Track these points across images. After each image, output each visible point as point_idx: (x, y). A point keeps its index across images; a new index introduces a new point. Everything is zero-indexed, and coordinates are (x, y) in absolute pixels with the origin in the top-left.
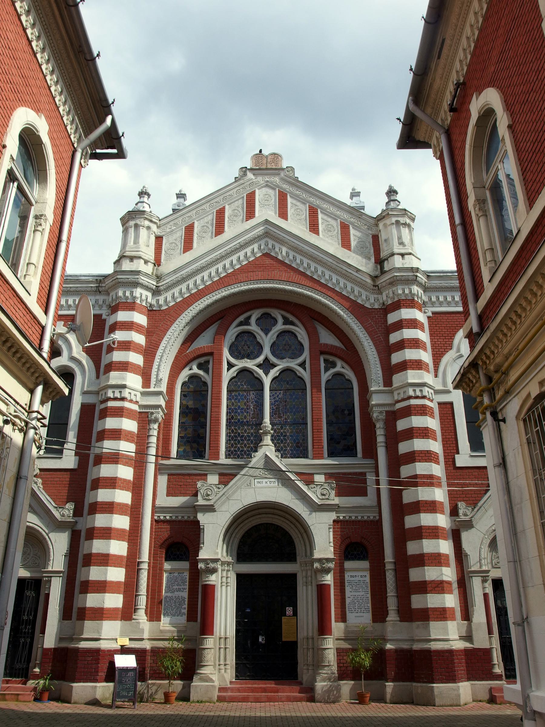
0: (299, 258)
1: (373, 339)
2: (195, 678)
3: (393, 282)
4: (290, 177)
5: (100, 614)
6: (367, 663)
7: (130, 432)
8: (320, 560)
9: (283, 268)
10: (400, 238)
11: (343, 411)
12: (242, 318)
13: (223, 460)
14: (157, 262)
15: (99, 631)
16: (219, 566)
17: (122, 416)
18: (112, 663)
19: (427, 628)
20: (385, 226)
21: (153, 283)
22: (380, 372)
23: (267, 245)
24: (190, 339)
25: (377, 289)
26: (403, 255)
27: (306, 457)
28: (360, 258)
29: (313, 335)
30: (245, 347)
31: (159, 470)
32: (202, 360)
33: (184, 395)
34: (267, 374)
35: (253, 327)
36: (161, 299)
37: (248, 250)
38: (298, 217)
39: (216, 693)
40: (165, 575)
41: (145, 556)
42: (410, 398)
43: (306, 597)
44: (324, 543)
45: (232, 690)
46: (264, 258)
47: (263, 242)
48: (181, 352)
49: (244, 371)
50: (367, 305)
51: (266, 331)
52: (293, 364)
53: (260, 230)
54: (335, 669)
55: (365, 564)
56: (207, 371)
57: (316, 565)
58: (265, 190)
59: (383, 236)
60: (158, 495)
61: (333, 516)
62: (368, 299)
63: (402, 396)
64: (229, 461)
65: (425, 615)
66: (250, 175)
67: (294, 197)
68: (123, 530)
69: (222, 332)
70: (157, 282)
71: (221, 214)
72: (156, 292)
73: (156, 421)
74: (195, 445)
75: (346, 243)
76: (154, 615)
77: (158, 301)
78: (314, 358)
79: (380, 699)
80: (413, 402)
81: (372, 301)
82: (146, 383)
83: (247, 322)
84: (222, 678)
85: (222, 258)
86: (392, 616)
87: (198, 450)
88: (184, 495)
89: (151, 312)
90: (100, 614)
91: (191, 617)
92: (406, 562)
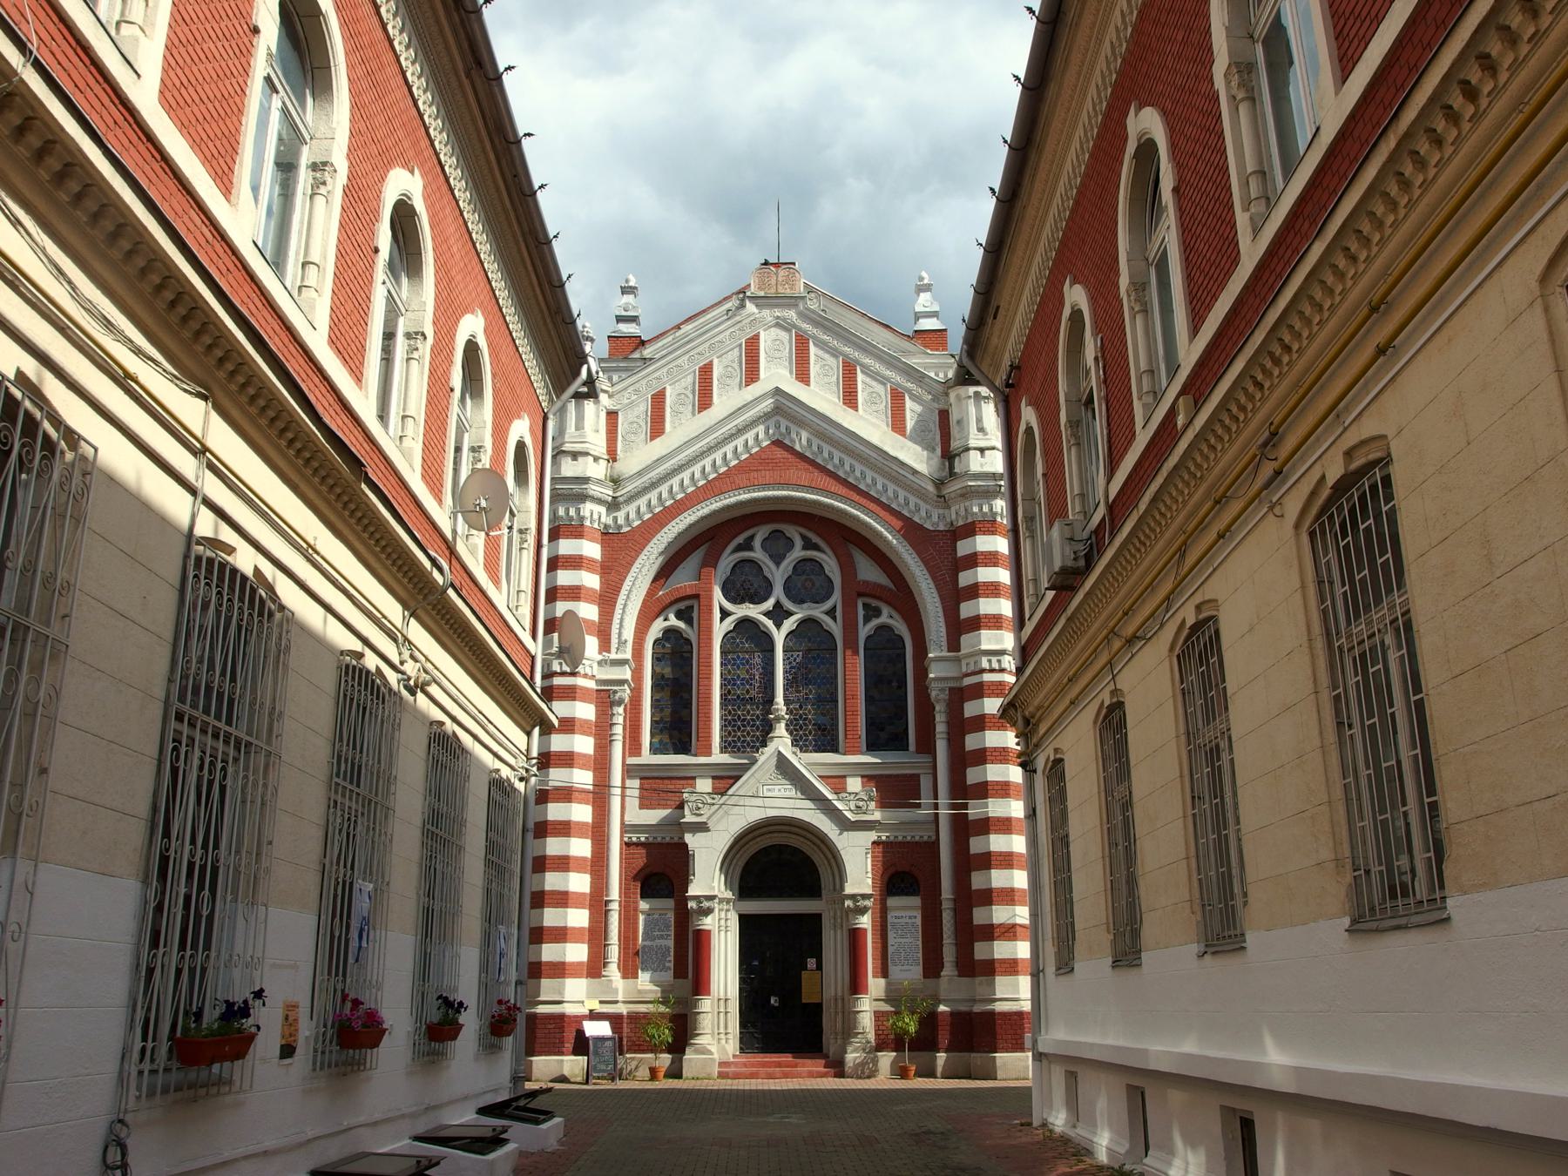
0: (826, 448)
1: (934, 578)
2: (688, 1050)
3: (967, 494)
4: (813, 312)
5: (560, 970)
6: (912, 1029)
7: (586, 721)
8: (853, 897)
9: (803, 465)
10: (979, 420)
11: (890, 682)
12: (740, 539)
13: (718, 757)
14: (612, 456)
15: (561, 993)
16: (715, 905)
17: (574, 699)
18: (580, 1033)
19: (992, 984)
20: (958, 397)
21: (607, 492)
22: (943, 630)
23: (778, 427)
24: (665, 572)
25: (943, 500)
26: (982, 450)
27: (835, 750)
28: (919, 448)
29: (848, 568)
30: (744, 587)
31: (629, 771)
32: (682, 605)
33: (657, 659)
34: (778, 625)
35: (758, 554)
36: (621, 515)
37: (750, 436)
38: (826, 380)
39: (716, 1069)
40: (641, 918)
41: (615, 893)
42: (983, 671)
43: (833, 944)
44: (859, 870)
45: (735, 1064)
46: (774, 448)
47: (771, 422)
48: (651, 593)
49: (745, 624)
50: (928, 526)
51: (778, 559)
52: (818, 612)
53: (767, 405)
54: (871, 1037)
55: (916, 901)
56: (689, 622)
57: (848, 903)
58: (775, 332)
59: (954, 417)
60: (630, 811)
61: (873, 836)
62: (929, 516)
63: (972, 668)
64: (726, 758)
65: (990, 969)
66: (750, 307)
67: (821, 345)
68: (584, 859)
69: (711, 561)
70: (615, 491)
71: (706, 372)
72: (613, 506)
73: (620, 702)
74: (676, 733)
75: (898, 425)
76: (629, 972)
77: (615, 519)
78: (849, 604)
79: (931, 1074)
80: (987, 677)
81: (935, 518)
82: (605, 646)
83: (747, 545)
84: (723, 1050)
85: (711, 449)
86: (948, 970)
87: (680, 740)
88: (665, 807)
89: (608, 537)
90: (560, 970)
91: (680, 972)
92: (972, 898)
